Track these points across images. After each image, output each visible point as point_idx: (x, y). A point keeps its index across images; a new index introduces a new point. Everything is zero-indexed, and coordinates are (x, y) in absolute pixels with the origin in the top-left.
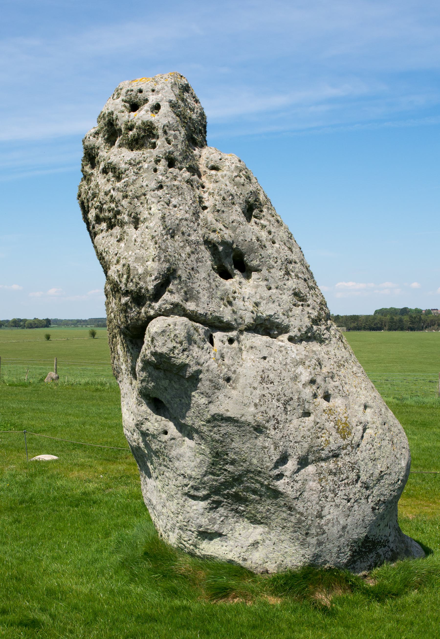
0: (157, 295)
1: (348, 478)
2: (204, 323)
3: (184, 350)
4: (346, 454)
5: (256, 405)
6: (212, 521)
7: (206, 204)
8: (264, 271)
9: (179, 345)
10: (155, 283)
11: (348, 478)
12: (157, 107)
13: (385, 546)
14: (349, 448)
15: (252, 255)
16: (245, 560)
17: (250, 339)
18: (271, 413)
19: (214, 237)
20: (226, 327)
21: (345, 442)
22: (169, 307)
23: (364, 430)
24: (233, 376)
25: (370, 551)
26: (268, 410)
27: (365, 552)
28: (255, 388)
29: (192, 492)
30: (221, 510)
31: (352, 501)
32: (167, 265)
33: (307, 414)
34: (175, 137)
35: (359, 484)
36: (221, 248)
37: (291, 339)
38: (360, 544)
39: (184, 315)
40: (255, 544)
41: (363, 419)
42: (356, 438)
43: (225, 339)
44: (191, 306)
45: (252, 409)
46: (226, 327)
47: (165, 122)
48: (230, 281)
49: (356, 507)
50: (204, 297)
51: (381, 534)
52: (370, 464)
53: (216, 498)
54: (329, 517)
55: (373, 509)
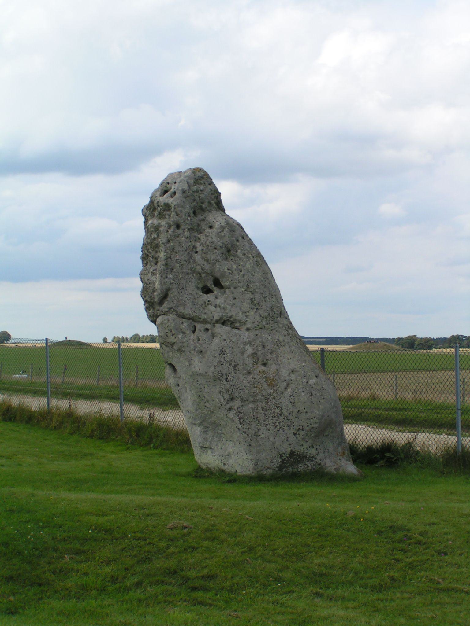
0: (161, 303)
1: (274, 412)
2: (189, 319)
3: (173, 335)
4: (273, 398)
5: (215, 366)
6: (206, 439)
7: (198, 250)
8: (232, 289)
9: (169, 332)
10: (159, 296)
11: (274, 412)
12: (175, 193)
13: (312, 461)
14: (275, 394)
15: (224, 280)
16: (224, 464)
17: (219, 329)
18: (224, 372)
19: (198, 268)
20: (205, 322)
21: (272, 391)
22: (166, 310)
23: (288, 385)
24: (204, 350)
25: (299, 462)
26: (222, 370)
27: (295, 462)
28: (215, 357)
29: (193, 422)
30: (210, 433)
31: (278, 427)
32: (164, 287)
33: (249, 373)
34: (181, 211)
35: (283, 417)
36: (203, 276)
37: (248, 329)
38: (288, 455)
39: (176, 315)
40: (229, 455)
41: (287, 378)
42: (280, 389)
43: (202, 329)
44: (181, 310)
45: (212, 369)
46: (205, 322)
47: (175, 203)
48: (210, 295)
49: (281, 431)
50: (189, 304)
51: (306, 452)
52: (290, 406)
53: (206, 424)
54: (263, 436)
55: (295, 434)
